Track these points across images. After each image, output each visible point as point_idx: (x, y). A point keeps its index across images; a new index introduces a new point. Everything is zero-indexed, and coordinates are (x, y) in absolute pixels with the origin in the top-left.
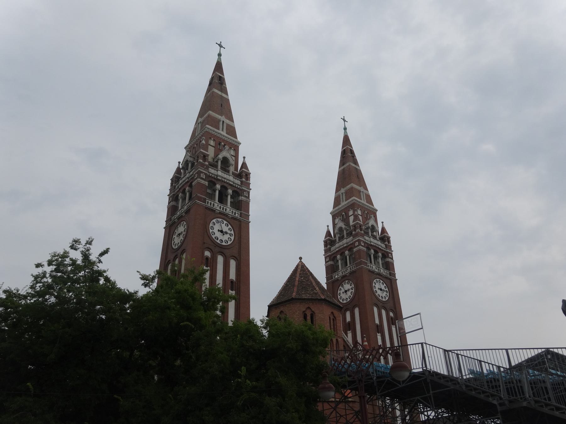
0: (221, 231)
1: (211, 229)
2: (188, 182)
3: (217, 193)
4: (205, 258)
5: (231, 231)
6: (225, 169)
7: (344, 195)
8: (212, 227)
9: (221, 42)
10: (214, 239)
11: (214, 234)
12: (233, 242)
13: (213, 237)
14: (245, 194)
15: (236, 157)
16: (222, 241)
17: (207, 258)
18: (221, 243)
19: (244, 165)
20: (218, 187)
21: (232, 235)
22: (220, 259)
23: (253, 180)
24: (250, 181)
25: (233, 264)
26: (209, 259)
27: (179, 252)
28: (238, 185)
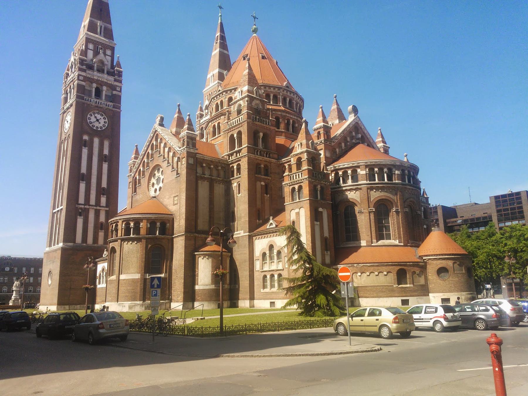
0: (98, 120)
1: (89, 119)
2: (72, 81)
3: (94, 90)
5: (105, 119)
6: (101, 70)
7: (212, 77)
8: (89, 118)
10: (92, 127)
12: (106, 128)
14: (118, 89)
15: (112, 56)
16: (98, 127)
17: (85, 141)
19: (119, 65)
20: (95, 85)
21: (106, 122)
22: (96, 141)
23: (124, 78)
24: (122, 77)
25: (106, 144)
27: (67, 135)
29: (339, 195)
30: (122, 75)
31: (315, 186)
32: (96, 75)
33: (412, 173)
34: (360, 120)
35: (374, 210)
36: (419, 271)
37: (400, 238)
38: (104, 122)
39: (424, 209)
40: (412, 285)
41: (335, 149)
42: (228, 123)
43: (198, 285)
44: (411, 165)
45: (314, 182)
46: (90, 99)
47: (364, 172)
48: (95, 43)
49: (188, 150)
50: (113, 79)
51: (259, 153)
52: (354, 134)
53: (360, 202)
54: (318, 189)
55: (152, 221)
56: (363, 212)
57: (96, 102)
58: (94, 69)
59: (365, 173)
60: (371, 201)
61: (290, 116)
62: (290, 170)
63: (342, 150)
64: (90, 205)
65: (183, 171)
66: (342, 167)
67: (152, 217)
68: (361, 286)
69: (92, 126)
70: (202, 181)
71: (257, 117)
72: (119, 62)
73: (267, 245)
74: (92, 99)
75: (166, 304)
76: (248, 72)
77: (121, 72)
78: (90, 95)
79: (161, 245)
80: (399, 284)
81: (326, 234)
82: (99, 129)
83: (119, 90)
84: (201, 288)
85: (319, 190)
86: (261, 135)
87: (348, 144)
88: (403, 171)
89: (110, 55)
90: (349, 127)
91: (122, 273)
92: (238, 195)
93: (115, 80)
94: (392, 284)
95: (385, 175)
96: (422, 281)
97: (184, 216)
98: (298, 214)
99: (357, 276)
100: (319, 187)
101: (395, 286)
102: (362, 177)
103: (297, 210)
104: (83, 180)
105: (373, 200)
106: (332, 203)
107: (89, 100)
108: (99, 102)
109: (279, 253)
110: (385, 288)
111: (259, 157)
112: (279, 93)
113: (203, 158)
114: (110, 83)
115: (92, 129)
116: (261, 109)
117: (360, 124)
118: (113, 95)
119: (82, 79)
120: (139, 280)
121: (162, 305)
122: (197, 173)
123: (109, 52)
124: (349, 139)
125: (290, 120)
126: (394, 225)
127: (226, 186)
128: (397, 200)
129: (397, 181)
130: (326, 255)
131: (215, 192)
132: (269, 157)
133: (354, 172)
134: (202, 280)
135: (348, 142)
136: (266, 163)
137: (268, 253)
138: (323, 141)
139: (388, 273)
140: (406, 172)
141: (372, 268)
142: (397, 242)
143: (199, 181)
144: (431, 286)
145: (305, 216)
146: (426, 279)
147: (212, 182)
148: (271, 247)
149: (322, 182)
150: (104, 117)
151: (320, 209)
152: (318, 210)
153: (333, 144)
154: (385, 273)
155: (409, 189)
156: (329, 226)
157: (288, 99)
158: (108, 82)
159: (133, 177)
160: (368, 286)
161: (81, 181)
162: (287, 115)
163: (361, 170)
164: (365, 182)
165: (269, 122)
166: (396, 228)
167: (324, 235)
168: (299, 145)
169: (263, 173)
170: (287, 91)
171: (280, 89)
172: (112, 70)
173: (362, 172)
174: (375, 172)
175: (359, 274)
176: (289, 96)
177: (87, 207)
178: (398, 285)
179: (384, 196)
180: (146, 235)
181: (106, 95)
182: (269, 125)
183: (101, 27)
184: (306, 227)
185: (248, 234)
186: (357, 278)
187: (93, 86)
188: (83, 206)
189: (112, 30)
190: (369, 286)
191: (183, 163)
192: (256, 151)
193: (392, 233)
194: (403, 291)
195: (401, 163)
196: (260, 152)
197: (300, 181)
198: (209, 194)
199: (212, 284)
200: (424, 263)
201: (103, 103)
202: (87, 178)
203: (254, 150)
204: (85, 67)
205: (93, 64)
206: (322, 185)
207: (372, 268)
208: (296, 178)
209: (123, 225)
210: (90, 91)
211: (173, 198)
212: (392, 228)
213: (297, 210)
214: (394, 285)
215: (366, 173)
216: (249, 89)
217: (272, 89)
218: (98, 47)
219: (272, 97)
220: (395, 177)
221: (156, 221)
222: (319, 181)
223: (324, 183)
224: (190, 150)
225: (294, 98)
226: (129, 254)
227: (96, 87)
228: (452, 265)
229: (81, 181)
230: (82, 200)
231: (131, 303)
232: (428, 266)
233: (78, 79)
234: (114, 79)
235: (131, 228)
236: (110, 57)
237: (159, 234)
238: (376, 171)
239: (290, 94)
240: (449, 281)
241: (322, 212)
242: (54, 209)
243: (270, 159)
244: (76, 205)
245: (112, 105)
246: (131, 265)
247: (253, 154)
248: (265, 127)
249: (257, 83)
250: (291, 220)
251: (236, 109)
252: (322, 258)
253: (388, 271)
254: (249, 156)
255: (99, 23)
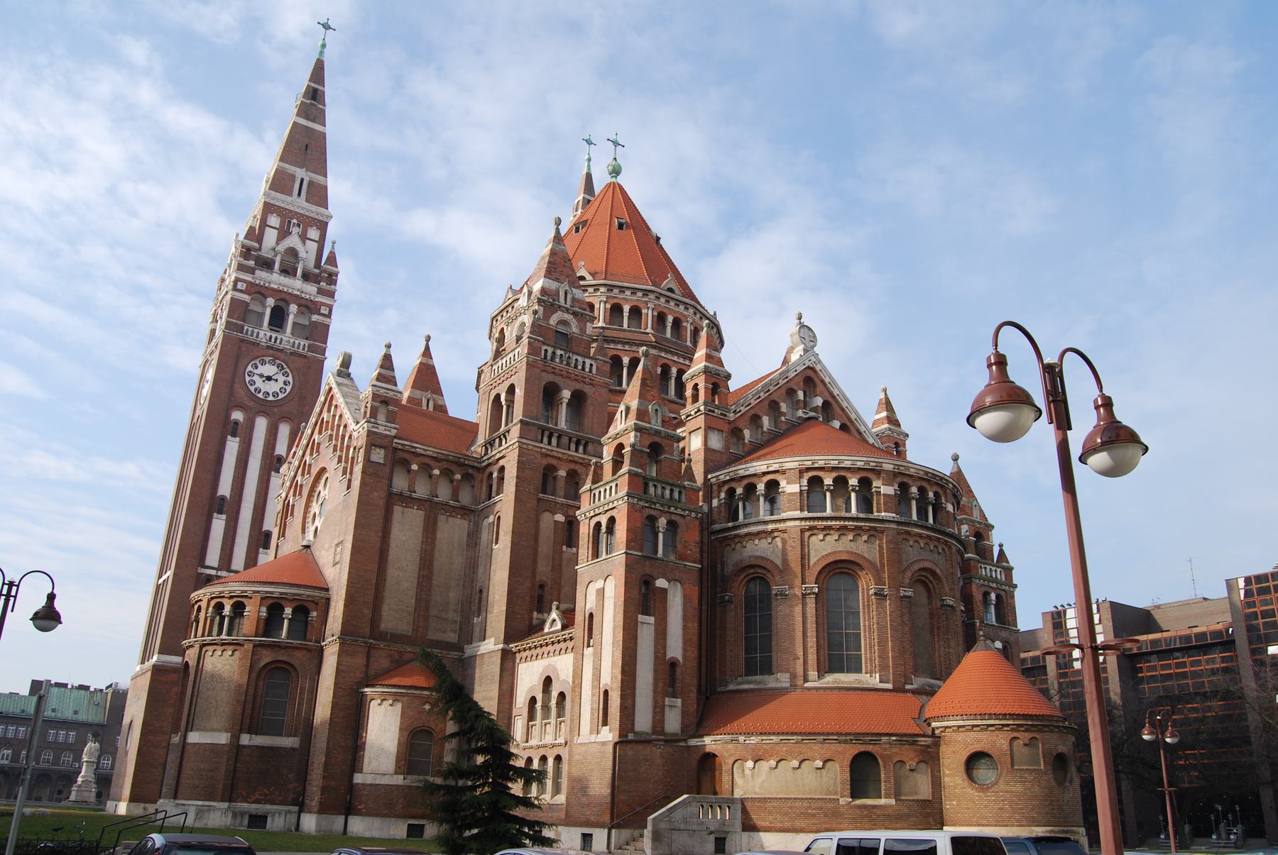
1: (249, 376)
4: (233, 422)
5: (288, 376)
6: (288, 271)
9: (328, 19)
11: (255, 383)
13: (252, 389)
14: (324, 310)
15: (321, 242)
16: (268, 394)
17: (236, 423)
18: (266, 397)
19: (332, 260)
20: (271, 302)
21: (289, 382)
22: (261, 424)
26: (239, 427)
28: (311, 295)
29: (733, 549)
30: (336, 281)
31: (652, 520)
32: (275, 279)
33: (931, 495)
34: (820, 362)
35: (817, 590)
36: (917, 760)
37: (883, 668)
38: (285, 383)
39: (998, 597)
40: (892, 801)
41: (741, 431)
42: (494, 367)
43: (362, 773)
44: (927, 473)
45: (646, 507)
46: (256, 331)
47: (795, 488)
48: (286, 215)
49: (373, 427)
50: (316, 289)
51: (554, 441)
52: (801, 395)
53: (781, 567)
54: (658, 527)
55: (271, 601)
56: (786, 595)
57: (271, 337)
58: (273, 269)
59: (799, 491)
60: (811, 564)
61: (669, 356)
62: (597, 479)
63: (763, 432)
64: (230, 571)
65: (356, 483)
66: (742, 473)
67: (272, 593)
68: (758, 798)
69: (256, 389)
70: (405, 507)
71: (559, 352)
72: (334, 253)
73: (540, 679)
74: (261, 332)
75: (288, 816)
76: (552, 250)
77: (337, 275)
78: (261, 325)
79: (292, 666)
80: (854, 795)
81: (675, 649)
82: (271, 398)
83: (326, 312)
84: (369, 779)
85: (660, 529)
86: (566, 394)
87: (783, 418)
88: (904, 487)
89: (317, 240)
90: (787, 377)
91: (194, 728)
92: (494, 545)
93: (320, 292)
94: (836, 793)
95: (853, 495)
96: (923, 788)
97: (343, 592)
98: (601, 592)
99: (743, 771)
100: (662, 522)
101: (843, 801)
102: (790, 501)
103: (599, 584)
104: (220, 512)
105: (815, 564)
106: (700, 566)
107: (255, 334)
108: (276, 339)
109: (562, 696)
110: (814, 805)
111: (552, 451)
112: (646, 303)
113: (414, 450)
114: (308, 297)
115: (253, 397)
116: (574, 333)
117: (820, 370)
118: (316, 324)
119: (244, 288)
120: (227, 749)
121: (277, 815)
122: (390, 485)
123: (313, 233)
124: (784, 407)
125: (670, 367)
126: (870, 631)
127: (472, 524)
128: (882, 564)
129: (883, 514)
130: (667, 709)
131: (439, 535)
132: (585, 453)
133: (773, 486)
134: (373, 761)
135: (784, 414)
136: (573, 466)
137: (539, 697)
138: (702, 408)
139: (825, 762)
140: (914, 490)
141: (784, 749)
142: (874, 680)
143: (396, 508)
144: (949, 806)
145: (615, 598)
146: (937, 784)
147: (432, 509)
148: (548, 681)
149: (672, 508)
150: (286, 372)
151: (661, 583)
152: (654, 584)
153: (732, 416)
154: (819, 763)
155: (920, 535)
156: (685, 628)
157: (670, 319)
158: (303, 295)
159: (285, 501)
160: (769, 798)
161: (215, 515)
162: (663, 354)
163: (788, 483)
164: (797, 514)
165: (591, 365)
166: (876, 640)
167: (665, 654)
168: (622, 411)
169: (562, 493)
170: (668, 299)
171: (649, 294)
172: (317, 271)
173: (790, 488)
174: (825, 488)
175: (750, 764)
176: (672, 311)
177: (224, 573)
178: (851, 800)
179: (848, 552)
180: (255, 637)
181: (294, 323)
182: (590, 371)
183: (302, 180)
184: (614, 628)
185: (501, 646)
186: (744, 776)
187: (267, 304)
188: (213, 572)
189: (326, 187)
190: (772, 798)
191: (360, 460)
192: (547, 433)
193: (866, 654)
194: (866, 816)
195: (897, 467)
196: (559, 437)
197: (611, 506)
198: (422, 542)
199: (396, 773)
200: (932, 739)
201: (286, 342)
202: (231, 508)
203: (540, 432)
204: (254, 262)
205: (274, 258)
206: (674, 518)
207: (784, 749)
208: (605, 498)
209: (211, 609)
210: (262, 315)
211: (334, 549)
212: (865, 640)
213: (599, 584)
214: (841, 799)
215: (801, 491)
216: (547, 285)
217: (628, 293)
218: (289, 222)
219: (626, 314)
220: (878, 504)
221: (283, 603)
222: (662, 505)
223: (679, 511)
224: (378, 428)
225: (686, 317)
226: (213, 682)
227: (275, 306)
228: (1006, 746)
229: (215, 515)
230: (213, 557)
231: (202, 806)
232: (943, 748)
233: (235, 288)
234: (318, 288)
235: (225, 616)
236: (316, 244)
237: (289, 635)
238: (827, 485)
239: (667, 302)
240: (998, 792)
241: (664, 591)
242: (160, 577)
243: (586, 457)
244: (197, 569)
245: (307, 345)
246: (213, 709)
247: (536, 441)
248: (577, 375)
249: (571, 273)
250: (587, 608)
251: (514, 335)
252: (654, 717)
253: (827, 756)
254: (524, 446)
255: (300, 173)
